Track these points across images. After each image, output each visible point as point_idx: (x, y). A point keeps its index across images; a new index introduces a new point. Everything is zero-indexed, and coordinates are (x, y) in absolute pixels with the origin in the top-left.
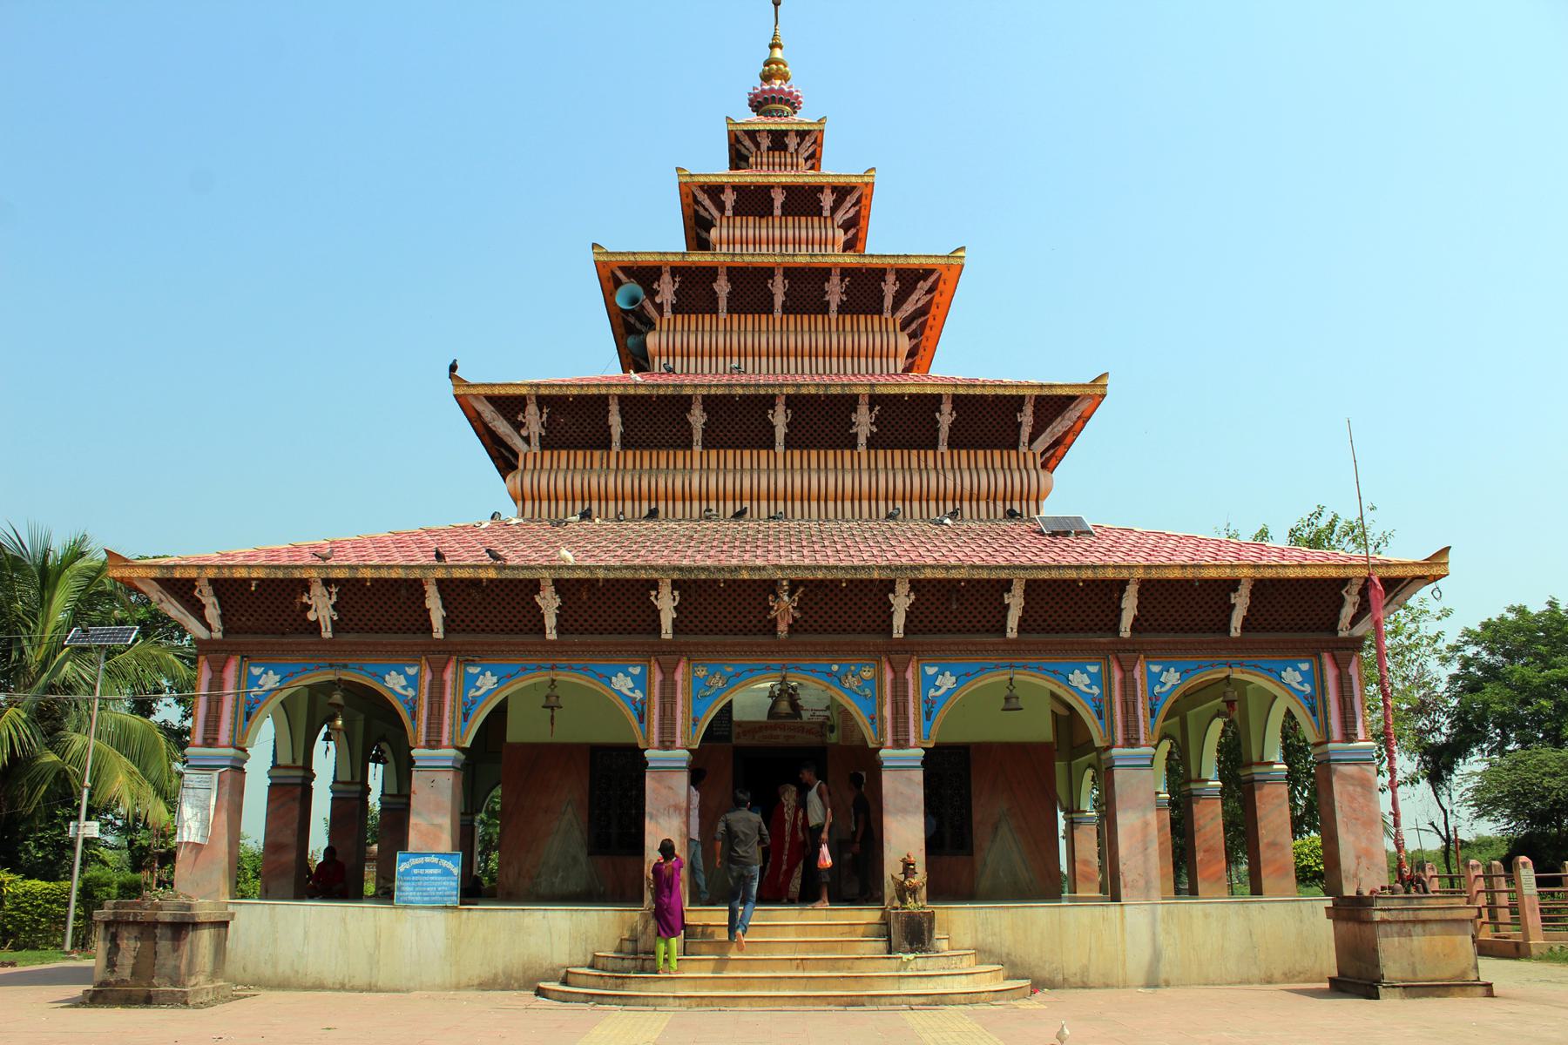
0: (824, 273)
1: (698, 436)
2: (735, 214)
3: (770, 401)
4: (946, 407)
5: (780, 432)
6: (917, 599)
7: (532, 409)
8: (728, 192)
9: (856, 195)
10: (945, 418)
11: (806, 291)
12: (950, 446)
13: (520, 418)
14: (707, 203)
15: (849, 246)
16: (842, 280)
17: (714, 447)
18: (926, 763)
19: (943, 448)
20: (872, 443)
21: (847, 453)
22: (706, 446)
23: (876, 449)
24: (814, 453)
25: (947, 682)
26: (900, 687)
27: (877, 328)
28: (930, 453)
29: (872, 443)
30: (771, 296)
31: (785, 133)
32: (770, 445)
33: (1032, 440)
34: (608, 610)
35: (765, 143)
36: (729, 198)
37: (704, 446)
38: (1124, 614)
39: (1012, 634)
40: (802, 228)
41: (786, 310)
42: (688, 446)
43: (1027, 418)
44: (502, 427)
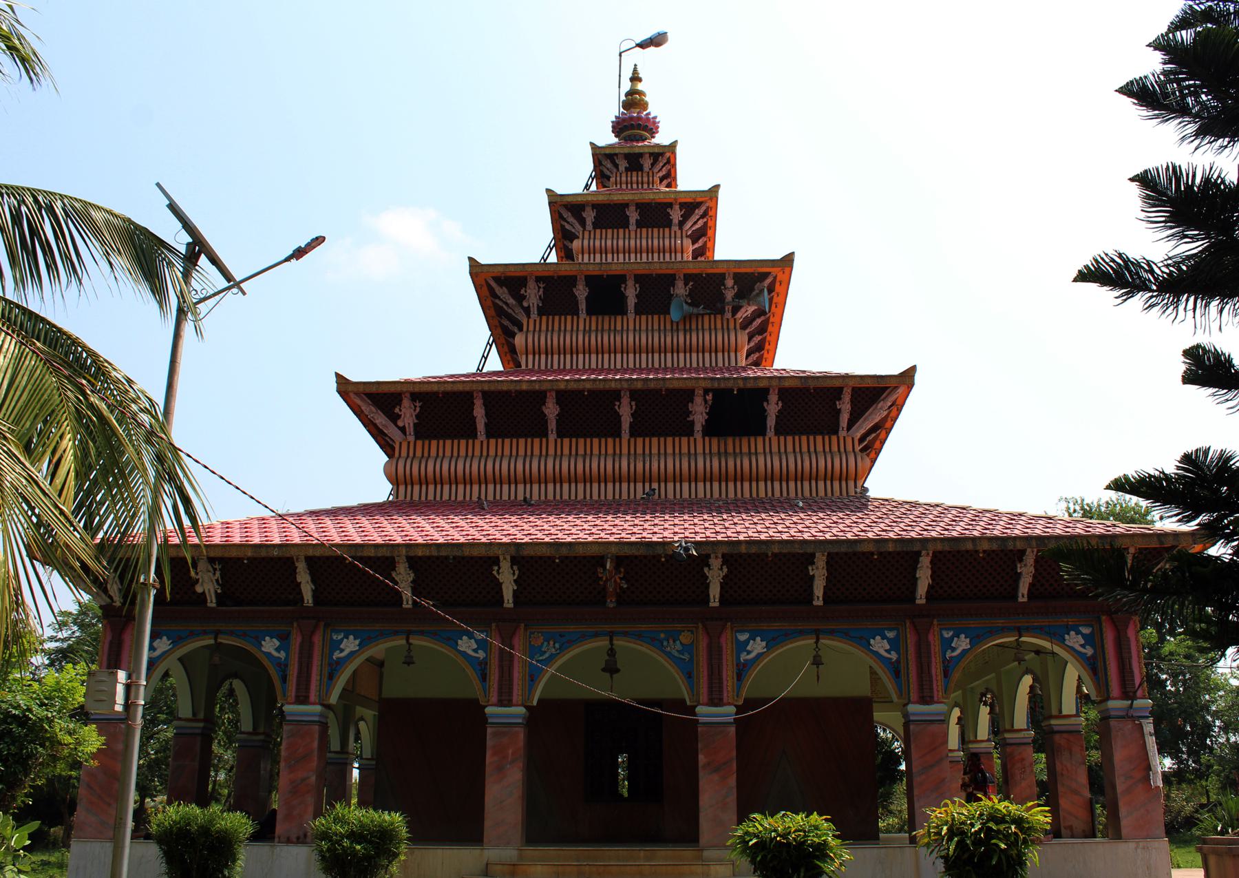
0: (670, 279)
1: (552, 425)
2: (595, 228)
3: (615, 395)
4: (773, 397)
6: (730, 571)
8: (589, 209)
9: (703, 208)
10: (773, 408)
11: (655, 292)
12: (778, 432)
13: (397, 410)
14: (571, 219)
15: (698, 253)
16: (686, 285)
18: (741, 725)
24: (655, 440)
25: (758, 646)
26: (715, 654)
27: (719, 326)
28: (760, 439)
30: (623, 298)
31: (641, 155)
34: (455, 577)
35: (623, 164)
36: (589, 216)
38: (919, 582)
39: (819, 602)
40: (655, 239)
41: (639, 311)
42: (543, 434)
44: (381, 420)
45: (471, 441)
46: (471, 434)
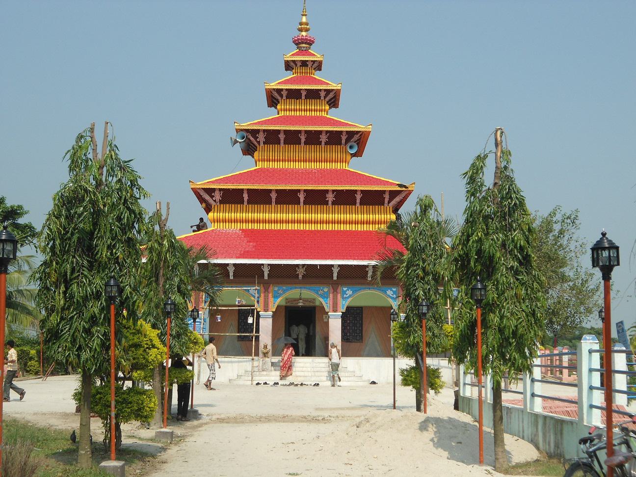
1: (274, 200)
5: (302, 200)
7: (217, 192)
13: (213, 194)
17: (279, 204)
19: (358, 205)
20: (334, 203)
21: (325, 206)
22: (277, 203)
23: (335, 205)
28: (354, 207)
29: (334, 203)
32: (299, 203)
33: (389, 202)
37: (276, 203)
43: (387, 196)
44: (207, 197)
45: (242, 205)
46: (242, 202)
